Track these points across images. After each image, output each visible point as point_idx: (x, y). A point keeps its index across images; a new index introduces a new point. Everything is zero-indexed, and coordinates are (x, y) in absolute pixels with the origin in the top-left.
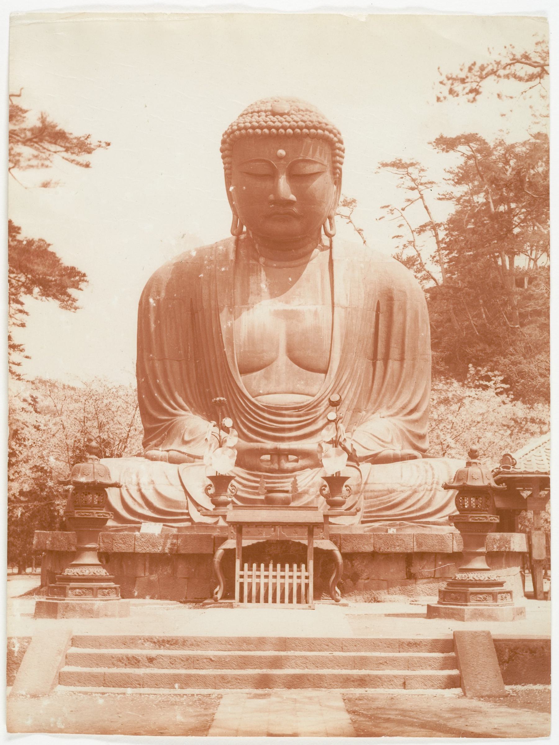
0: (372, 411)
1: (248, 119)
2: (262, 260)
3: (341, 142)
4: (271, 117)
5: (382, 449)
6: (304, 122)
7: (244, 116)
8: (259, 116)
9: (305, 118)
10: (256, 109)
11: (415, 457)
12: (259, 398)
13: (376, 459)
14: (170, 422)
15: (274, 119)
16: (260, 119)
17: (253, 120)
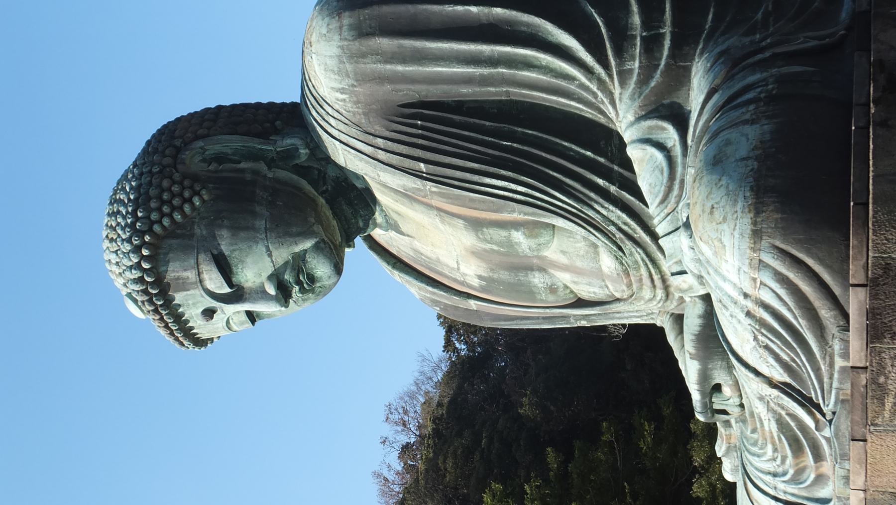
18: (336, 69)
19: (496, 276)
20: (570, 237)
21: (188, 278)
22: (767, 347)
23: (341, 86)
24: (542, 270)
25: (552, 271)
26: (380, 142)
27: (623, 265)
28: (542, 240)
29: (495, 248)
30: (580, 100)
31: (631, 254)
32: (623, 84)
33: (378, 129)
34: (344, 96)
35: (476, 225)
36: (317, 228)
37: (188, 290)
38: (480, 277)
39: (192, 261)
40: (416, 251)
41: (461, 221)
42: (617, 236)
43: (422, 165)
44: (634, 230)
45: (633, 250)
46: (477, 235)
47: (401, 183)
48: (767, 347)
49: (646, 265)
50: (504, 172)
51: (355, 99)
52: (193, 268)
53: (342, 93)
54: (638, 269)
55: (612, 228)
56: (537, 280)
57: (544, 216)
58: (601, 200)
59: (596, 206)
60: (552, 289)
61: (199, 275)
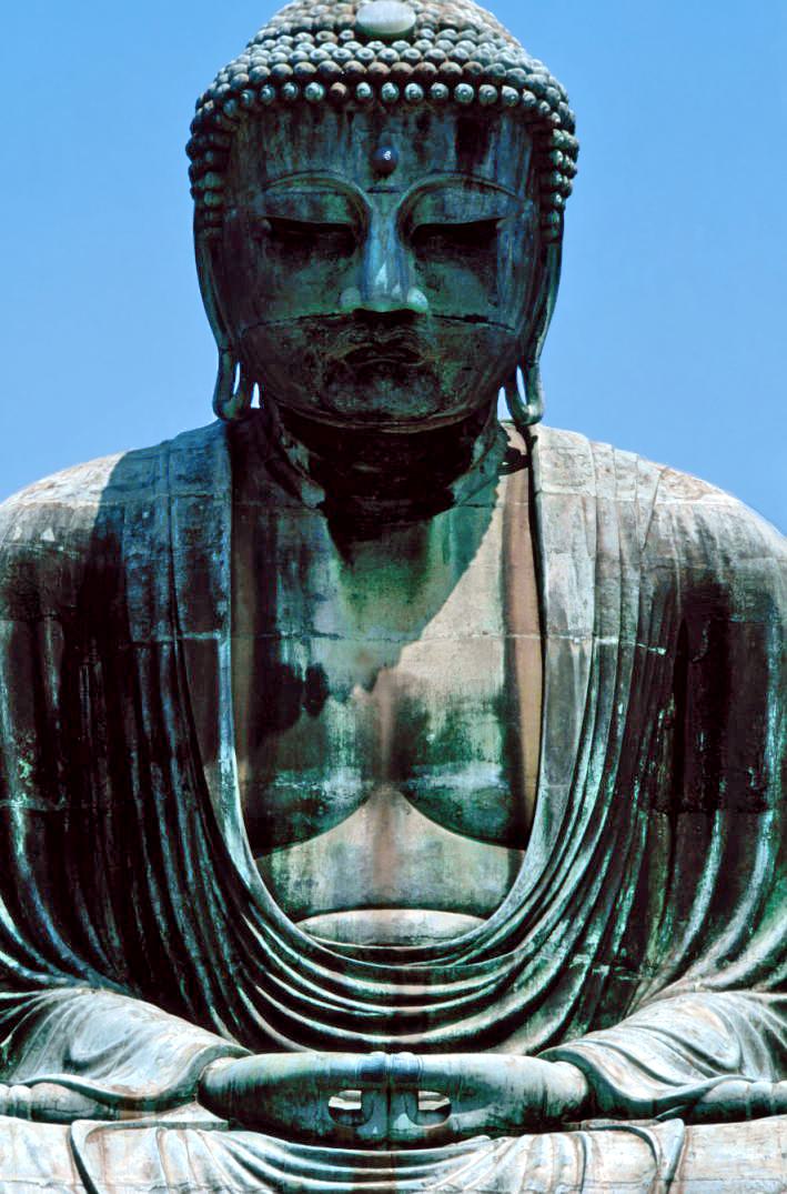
0: (665, 974)
1: (281, 52)
2: (313, 495)
3: (568, 125)
4: (356, 45)
5: (707, 1082)
6: (461, 62)
7: (270, 42)
8: (317, 44)
9: (458, 51)
10: (308, 21)
12: (312, 922)
13: (693, 1110)
14: (18, 1009)
15: (363, 51)
16: (322, 51)
17: (300, 53)
18: (744, 536)
20: (487, 867)
21: (481, 162)
23: (716, 536)
24: (363, 799)
25: (362, 814)
26: (633, 576)
27: (446, 955)
30: (705, 926)
31: (481, 972)
34: (694, 537)
35: (506, 708)
36: (463, 407)
37: (459, 150)
39: (503, 181)
40: (306, 556)
42: (516, 951)
43: (614, 640)
44: (525, 983)
45: (491, 977)
46: (469, 699)
47: (565, 589)
49: (459, 994)
50: (612, 778)
51: (695, 554)
52: (495, 180)
53: (699, 532)
54: (446, 979)
55: (528, 944)
56: (341, 782)
57: (548, 830)
58: (573, 936)
59: (563, 926)
61: (483, 188)
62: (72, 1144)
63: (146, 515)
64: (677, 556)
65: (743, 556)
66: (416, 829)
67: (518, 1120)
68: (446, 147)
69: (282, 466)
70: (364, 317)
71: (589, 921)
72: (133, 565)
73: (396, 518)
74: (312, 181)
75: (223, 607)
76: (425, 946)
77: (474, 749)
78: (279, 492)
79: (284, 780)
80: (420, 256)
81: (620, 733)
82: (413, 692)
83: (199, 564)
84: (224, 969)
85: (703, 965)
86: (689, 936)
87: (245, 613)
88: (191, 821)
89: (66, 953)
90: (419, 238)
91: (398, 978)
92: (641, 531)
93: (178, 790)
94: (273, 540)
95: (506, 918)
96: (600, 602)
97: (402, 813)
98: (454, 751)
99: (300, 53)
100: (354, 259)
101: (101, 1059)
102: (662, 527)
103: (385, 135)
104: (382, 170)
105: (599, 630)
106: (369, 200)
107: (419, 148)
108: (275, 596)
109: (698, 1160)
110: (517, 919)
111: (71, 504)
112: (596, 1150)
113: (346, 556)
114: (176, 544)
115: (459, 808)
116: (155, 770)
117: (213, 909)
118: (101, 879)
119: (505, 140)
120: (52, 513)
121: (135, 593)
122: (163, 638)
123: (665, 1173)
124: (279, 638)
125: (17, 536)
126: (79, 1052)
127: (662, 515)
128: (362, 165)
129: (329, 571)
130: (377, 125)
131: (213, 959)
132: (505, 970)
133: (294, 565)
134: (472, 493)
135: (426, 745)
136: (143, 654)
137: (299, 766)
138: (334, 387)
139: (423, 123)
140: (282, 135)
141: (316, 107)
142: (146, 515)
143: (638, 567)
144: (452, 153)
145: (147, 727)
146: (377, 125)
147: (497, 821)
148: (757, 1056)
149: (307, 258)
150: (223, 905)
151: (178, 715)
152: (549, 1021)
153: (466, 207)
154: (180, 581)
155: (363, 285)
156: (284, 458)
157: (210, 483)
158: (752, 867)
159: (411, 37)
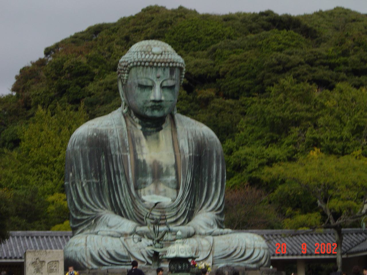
2: (139, 127)
11: (231, 233)
16: (147, 56)
19: (148, 165)
21: (173, 75)
22: (235, 250)
24: (153, 182)
26: (193, 143)
28: (171, 185)
29: (164, 169)
30: (204, 201)
31: (173, 211)
32: (217, 214)
33: (196, 144)
35: (176, 166)
38: (144, 161)
40: (140, 139)
41: (174, 161)
44: (180, 213)
48: (235, 250)
54: (168, 212)
60: (145, 183)
61: (174, 80)
62: (122, 242)
63: (112, 131)
64: (199, 138)
65: (210, 138)
66: (162, 187)
67: (186, 236)
68: (168, 74)
69: (133, 122)
70: (154, 101)
71: (189, 201)
72: (111, 141)
73: (153, 132)
74: (146, 78)
75: (128, 149)
76: (165, 207)
77: (171, 173)
78: (133, 126)
79: (140, 179)
80: (163, 90)
81: (193, 170)
82: (160, 164)
83: (123, 141)
84: (131, 210)
85: (204, 208)
86: (202, 203)
87: (132, 150)
88: (124, 186)
89: (101, 206)
90: (162, 87)
91: (161, 212)
92: (194, 134)
93: (122, 181)
94: (134, 137)
95: (177, 202)
96: (189, 148)
97: (159, 185)
98: (168, 174)
99: (143, 56)
100: (153, 90)
101: (115, 226)
102: (197, 134)
103: (158, 71)
104: (158, 77)
105: (189, 152)
106: (156, 82)
107: (164, 74)
108: (136, 147)
109: (216, 243)
110: (179, 202)
111: (98, 128)
112: (200, 242)
113: (146, 138)
114: (119, 137)
115: (169, 184)
116: (117, 176)
117: (129, 200)
118: (105, 193)
119: (177, 71)
120: (95, 130)
121: (112, 146)
122: (118, 153)
123: (212, 245)
124: (137, 154)
125: (89, 134)
126: (110, 224)
127: (197, 132)
128: (155, 76)
129: (144, 141)
130: (157, 70)
131: (129, 208)
132: (177, 211)
133: (138, 141)
134: (165, 127)
135: (163, 173)
136: (114, 157)
137: (143, 176)
138: (147, 112)
139: (164, 69)
140: (141, 70)
141: (147, 67)
142: (112, 131)
143: (194, 141)
144: (169, 74)
145: (115, 169)
146: (157, 70)
147: (175, 186)
148: (215, 223)
149: (145, 90)
150: (131, 200)
151: (121, 167)
152: (183, 218)
153: (170, 83)
154: (120, 144)
155: (155, 96)
156: (133, 120)
157: (123, 126)
158: (211, 191)
159: (162, 54)
